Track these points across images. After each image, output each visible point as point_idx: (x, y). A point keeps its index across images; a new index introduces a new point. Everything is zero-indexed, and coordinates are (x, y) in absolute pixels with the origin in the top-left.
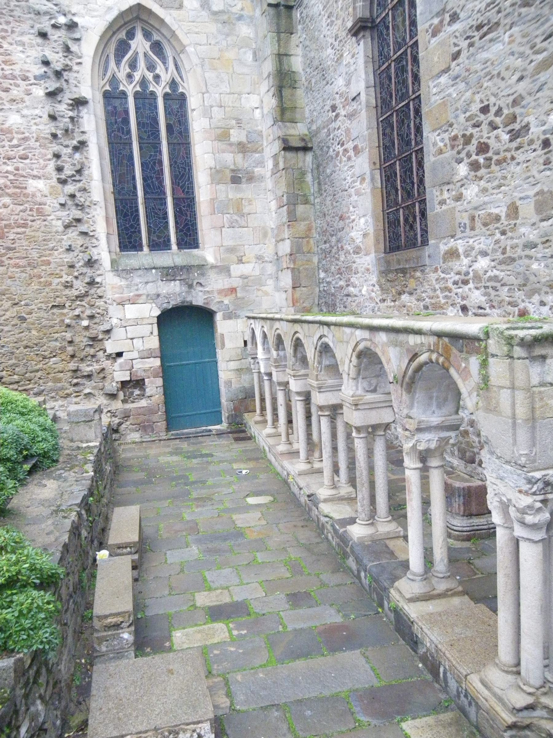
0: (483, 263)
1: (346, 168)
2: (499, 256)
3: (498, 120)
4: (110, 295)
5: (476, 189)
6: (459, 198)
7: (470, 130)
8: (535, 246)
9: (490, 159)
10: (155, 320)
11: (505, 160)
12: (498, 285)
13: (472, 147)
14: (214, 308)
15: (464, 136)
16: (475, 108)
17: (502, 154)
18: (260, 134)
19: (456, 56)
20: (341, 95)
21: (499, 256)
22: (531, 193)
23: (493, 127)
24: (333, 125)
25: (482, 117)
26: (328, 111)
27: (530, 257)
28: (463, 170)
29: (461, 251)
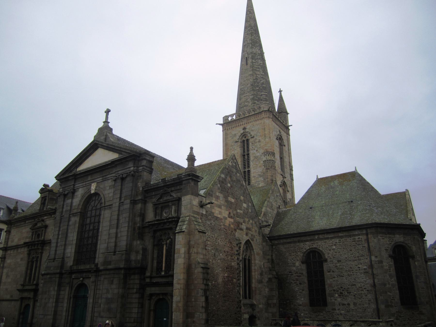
0: (342, 312)
1: (296, 286)
2: (346, 311)
3: (344, 290)
4: (243, 311)
5: (340, 299)
6: (336, 300)
7: (338, 290)
8: (354, 310)
9: (343, 295)
10: (248, 319)
11: (346, 296)
12: (346, 316)
13: (339, 292)
14: (257, 317)
15: (337, 290)
16: (339, 287)
17: (346, 295)
18: (263, 271)
19: (335, 277)
20: (294, 271)
21: (346, 311)
22: (353, 302)
23: (343, 290)
24: (290, 276)
25: (341, 288)
26: (288, 272)
27: (353, 312)
28: (337, 295)
29: (337, 309)
